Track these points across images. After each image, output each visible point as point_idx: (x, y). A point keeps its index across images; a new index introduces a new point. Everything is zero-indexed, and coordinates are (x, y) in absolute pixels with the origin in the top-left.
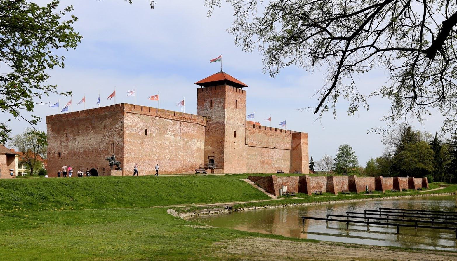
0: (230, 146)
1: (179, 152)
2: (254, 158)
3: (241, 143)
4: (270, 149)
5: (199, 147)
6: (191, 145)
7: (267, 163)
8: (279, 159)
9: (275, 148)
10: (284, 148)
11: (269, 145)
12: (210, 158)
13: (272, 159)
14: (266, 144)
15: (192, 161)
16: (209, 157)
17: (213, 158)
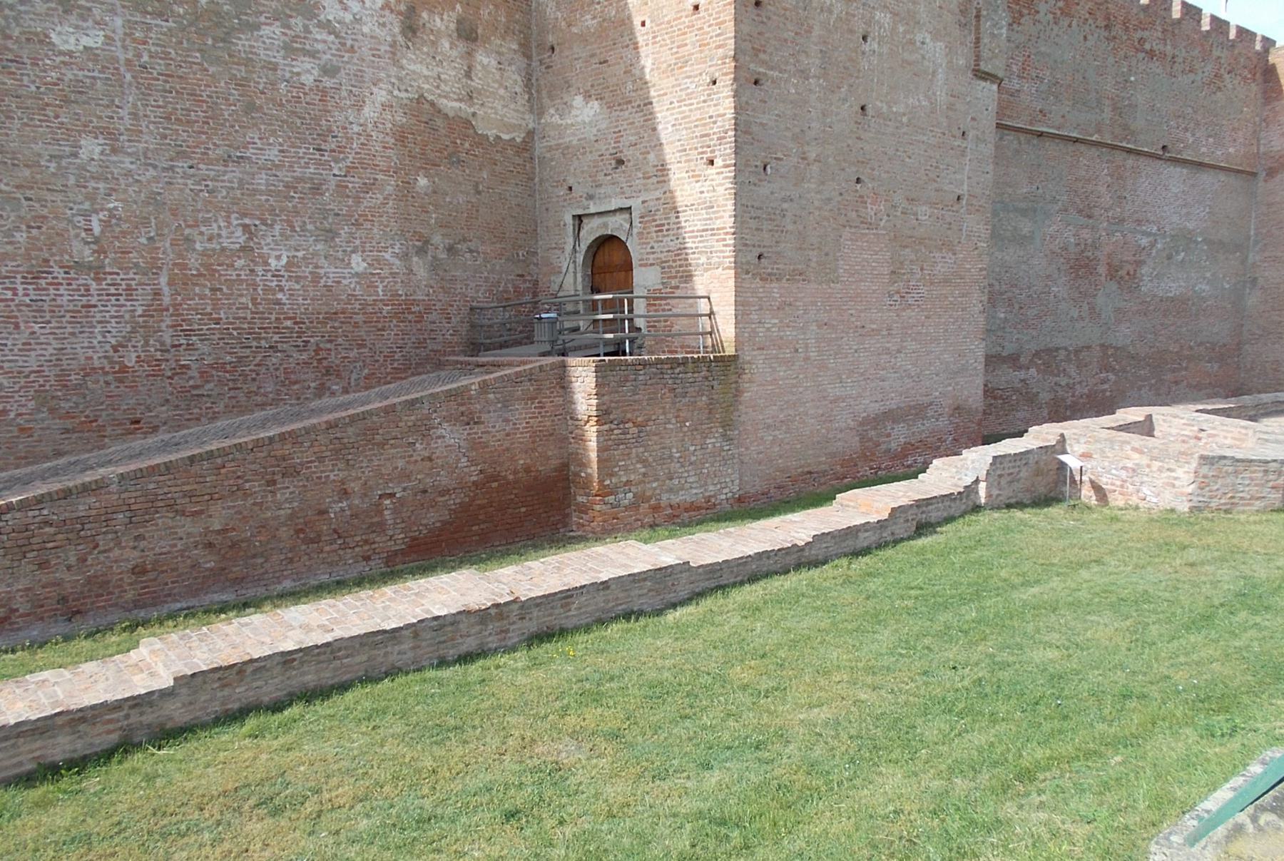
0: (813, 63)
1: (91, 148)
2: (1026, 227)
3: (936, 50)
4: (1131, 161)
5: (450, 105)
6: (308, 72)
7: (1113, 272)
8: (1184, 239)
9: (1165, 155)
10: (1218, 156)
11: (1125, 127)
12: (592, 230)
13: (1144, 241)
14: (1107, 114)
15: (329, 271)
16: (579, 219)
17: (616, 225)
